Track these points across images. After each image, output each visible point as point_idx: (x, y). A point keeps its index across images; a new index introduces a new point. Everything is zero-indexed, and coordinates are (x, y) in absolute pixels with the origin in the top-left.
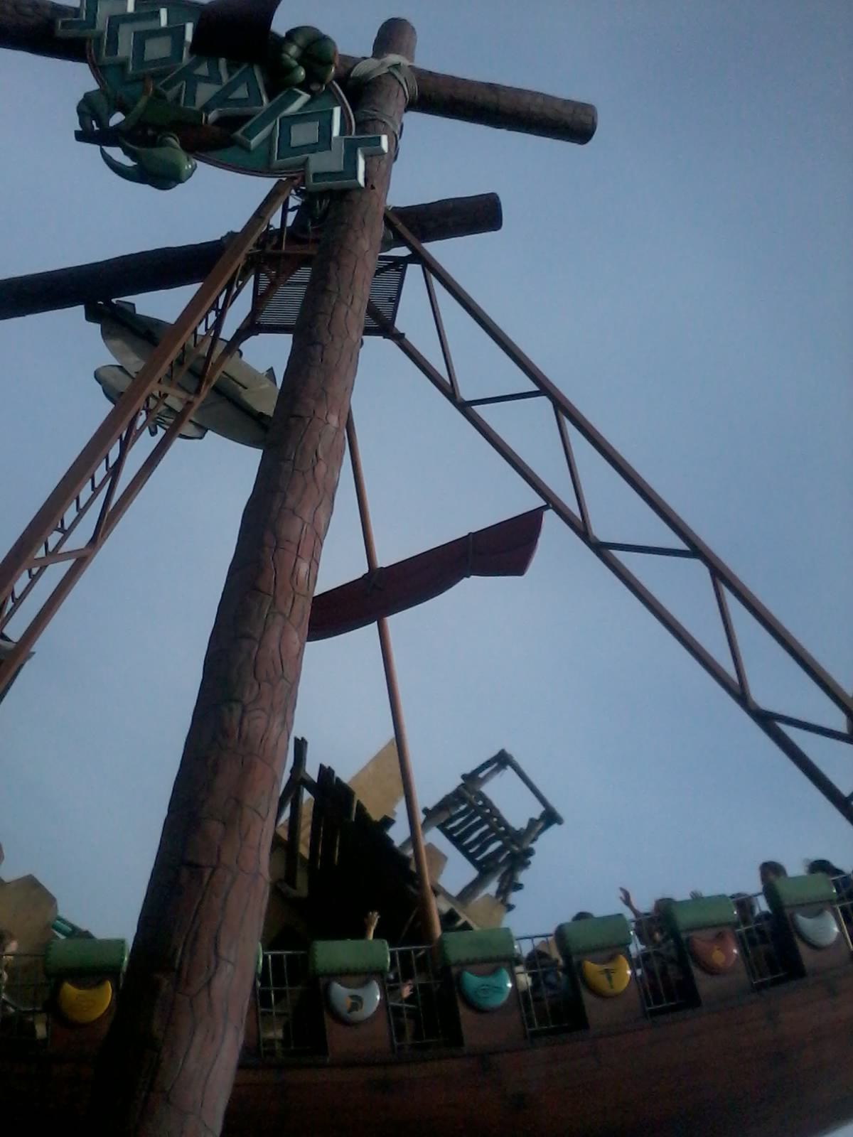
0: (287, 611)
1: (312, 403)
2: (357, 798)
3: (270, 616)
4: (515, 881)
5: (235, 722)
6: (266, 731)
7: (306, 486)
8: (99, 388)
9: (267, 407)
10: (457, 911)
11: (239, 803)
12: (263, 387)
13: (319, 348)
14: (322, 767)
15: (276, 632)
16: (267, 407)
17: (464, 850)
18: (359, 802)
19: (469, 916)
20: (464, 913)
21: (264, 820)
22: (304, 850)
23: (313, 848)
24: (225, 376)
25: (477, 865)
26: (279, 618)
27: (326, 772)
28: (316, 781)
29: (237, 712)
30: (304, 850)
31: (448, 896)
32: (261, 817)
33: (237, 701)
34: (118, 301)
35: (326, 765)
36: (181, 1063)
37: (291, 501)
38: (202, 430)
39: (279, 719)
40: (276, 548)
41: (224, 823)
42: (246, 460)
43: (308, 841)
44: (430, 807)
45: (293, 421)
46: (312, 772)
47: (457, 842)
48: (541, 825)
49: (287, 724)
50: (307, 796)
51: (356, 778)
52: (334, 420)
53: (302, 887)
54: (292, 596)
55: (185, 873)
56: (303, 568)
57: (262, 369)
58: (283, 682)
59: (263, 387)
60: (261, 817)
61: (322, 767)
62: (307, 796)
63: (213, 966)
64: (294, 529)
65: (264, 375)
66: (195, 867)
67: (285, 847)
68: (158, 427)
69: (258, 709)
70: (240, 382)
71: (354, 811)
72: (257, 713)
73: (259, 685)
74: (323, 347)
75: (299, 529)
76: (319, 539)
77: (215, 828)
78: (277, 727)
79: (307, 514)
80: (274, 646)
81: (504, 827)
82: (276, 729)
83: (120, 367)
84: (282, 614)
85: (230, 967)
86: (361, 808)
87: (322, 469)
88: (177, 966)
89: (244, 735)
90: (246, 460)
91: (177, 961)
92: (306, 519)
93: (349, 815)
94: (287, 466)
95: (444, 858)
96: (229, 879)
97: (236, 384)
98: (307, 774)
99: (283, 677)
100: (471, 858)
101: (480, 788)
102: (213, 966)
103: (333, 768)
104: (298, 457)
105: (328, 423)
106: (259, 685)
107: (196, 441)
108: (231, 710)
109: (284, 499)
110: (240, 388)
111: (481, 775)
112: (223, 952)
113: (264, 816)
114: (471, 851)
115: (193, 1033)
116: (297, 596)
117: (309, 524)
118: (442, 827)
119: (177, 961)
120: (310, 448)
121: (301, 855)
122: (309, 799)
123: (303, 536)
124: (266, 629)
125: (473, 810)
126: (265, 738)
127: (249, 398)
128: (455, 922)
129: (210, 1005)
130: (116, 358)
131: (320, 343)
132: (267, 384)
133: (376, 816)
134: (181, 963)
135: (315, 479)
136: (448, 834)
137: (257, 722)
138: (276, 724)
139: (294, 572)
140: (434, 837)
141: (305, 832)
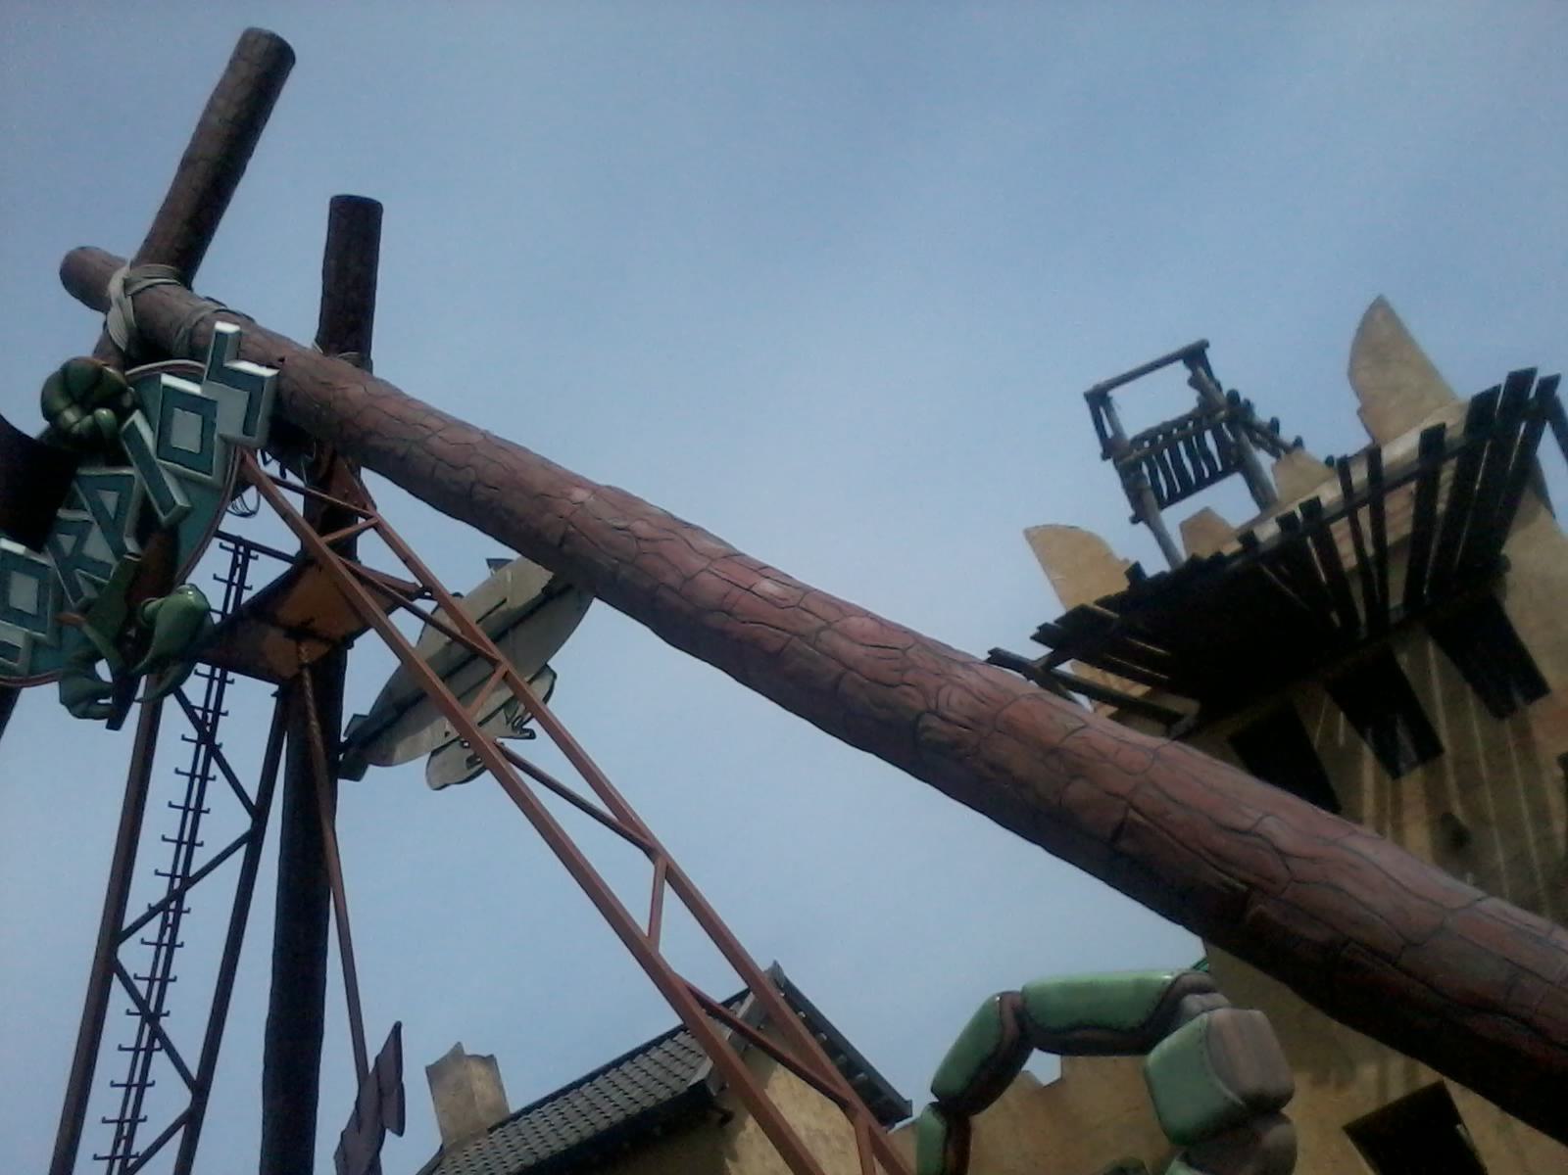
0: (819, 623)
5: (945, 727)
7: (659, 555)
9: (538, 578)
10: (1280, 514)
11: (1054, 751)
13: (479, 488)
14: (1035, 638)
15: (843, 645)
16: (538, 578)
17: (1202, 483)
18: (1098, 603)
22: (1138, 690)
25: (1226, 472)
26: (825, 635)
27: (1044, 635)
28: (1050, 650)
30: (1138, 690)
33: (919, 716)
34: (345, 735)
35: (1034, 631)
37: (671, 579)
38: (544, 671)
39: (959, 671)
40: (729, 613)
42: (601, 617)
43: (1127, 682)
44: (1131, 512)
45: (566, 548)
46: (1037, 652)
47: (1189, 489)
48: (1201, 371)
49: (967, 662)
50: (1066, 668)
51: (1062, 599)
53: (1186, 706)
55: (1125, 844)
56: (767, 587)
57: (486, 573)
60: (1083, 727)
61: (1035, 638)
62: (1066, 668)
63: (1257, 840)
64: (711, 585)
66: (1120, 830)
67: (1127, 710)
68: (525, 727)
69: (937, 694)
72: (944, 693)
76: (732, 556)
77: (1078, 790)
79: (697, 563)
80: (860, 651)
81: (1190, 420)
82: (970, 678)
83: (435, 753)
84: (822, 629)
86: (1105, 602)
87: (641, 528)
88: (1244, 887)
89: (966, 722)
90: (601, 617)
91: (1238, 885)
94: (625, 572)
99: (904, 651)
100: (1216, 477)
103: (1040, 623)
105: (582, 503)
108: (928, 728)
109: (670, 588)
110: (503, 608)
111: (1110, 432)
112: (1246, 824)
113: (1082, 724)
114: (1207, 474)
115: (1338, 889)
116: (802, 605)
117: (710, 564)
118: (1163, 504)
119: (1238, 885)
122: (1072, 666)
123: (724, 576)
125: (1154, 457)
127: (519, 600)
129: (1312, 859)
130: (420, 756)
131: (473, 484)
132: (507, 573)
133: (1122, 585)
134: (1242, 882)
136: (1174, 498)
137: (955, 701)
140: (1173, 517)
141: (1114, 682)
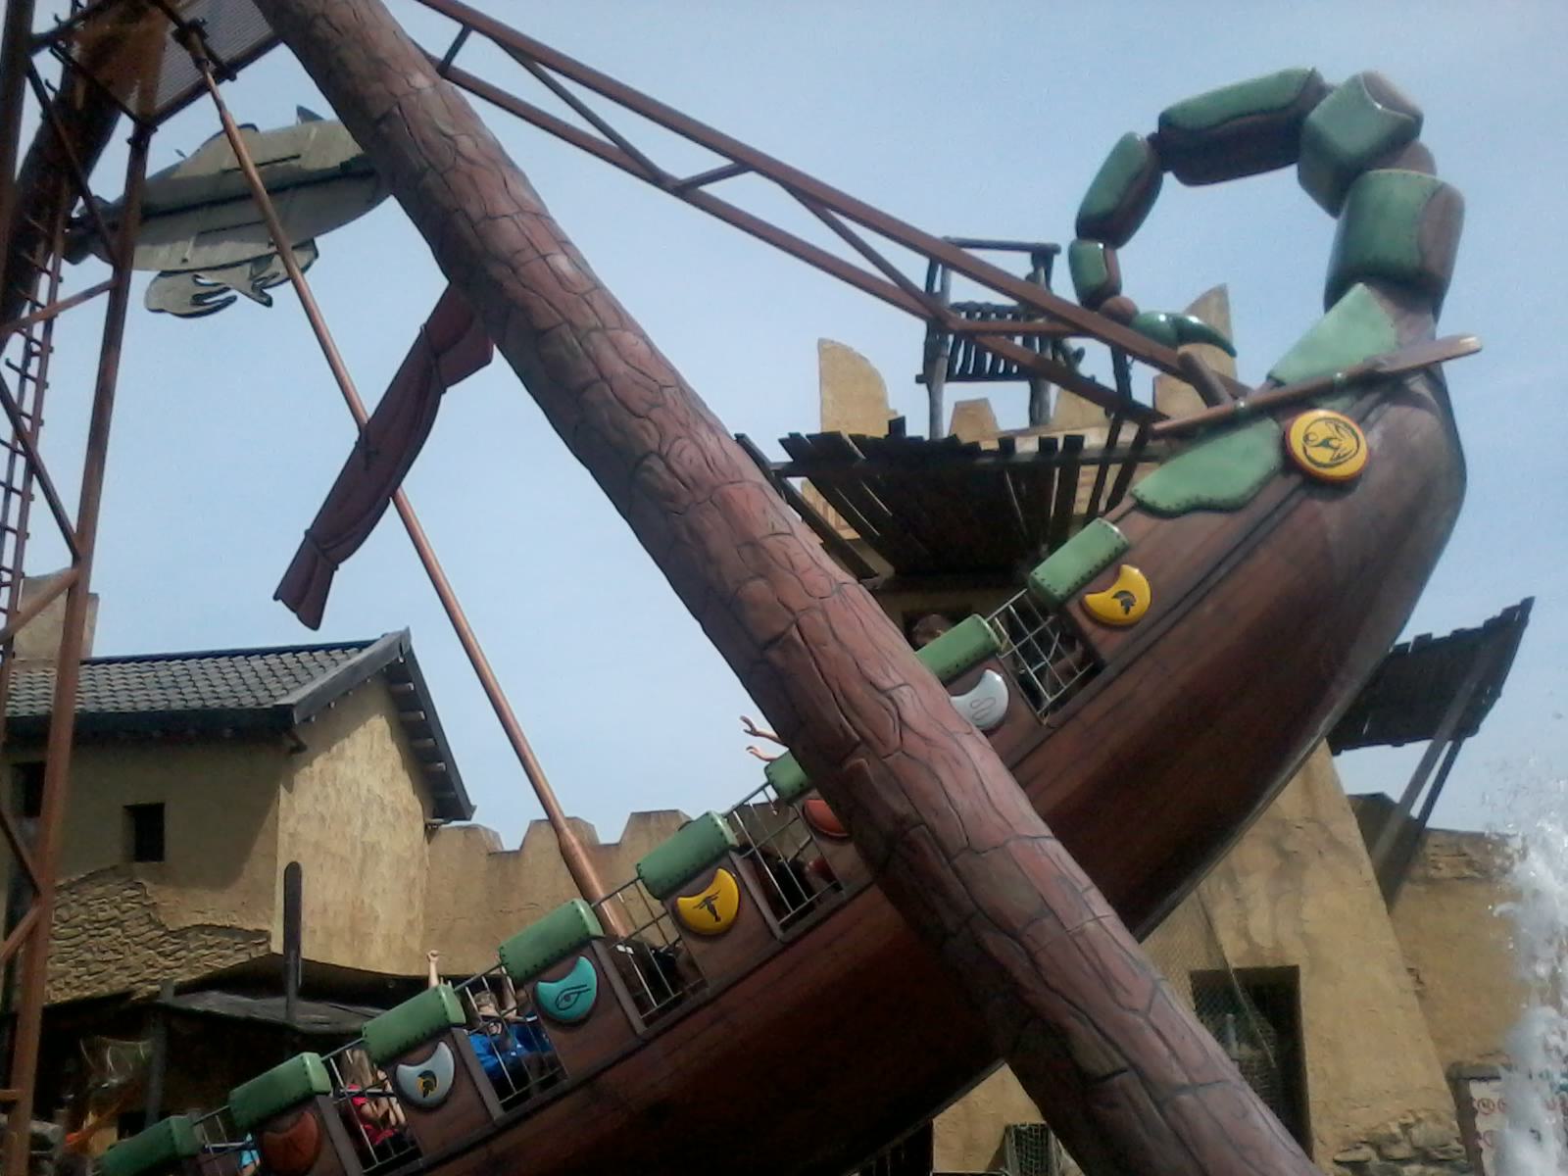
0: (593, 321)
1: (377, 88)
2: (846, 436)
3: (585, 344)
4: (1071, 353)
5: (666, 476)
6: (702, 451)
7: (470, 177)
8: (167, 317)
9: (345, 148)
10: (1045, 435)
11: (753, 544)
12: (313, 136)
13: (321, 23)
14: (782, 442)
15: (608, 354)
16: (345, 148)
17: (993, 376)
18: (851, 436)
19: (1062, 430)
20: (1054, 431)
21: (791, 534)
22: (848, 534)
23: (854, 523)
24: (263, 168)
25: (1018, 377)
26: (595, 336)
27: (791, 443)
28: (790, 460)
29: (659, 466)
30: (848, 534)
31: (1023, 433)
32: (789, 534)
33: (646, 456)
34: (78, 212)
35: (785, 435)
36: (952, 811)
37: (474, 210)
38: (308, 245)
39: (703, 431)
40: (515, 271)
41: (762, 576)
42: (389, 218)
43: (843, 522)
44: (920, 371)
45: (384, 128)
46: (778, 456)
47: (979, 375)
48: (1042, 272)
49: (715, 427)
50: (797, 483)
51: (823, 419)
52: (421, 81)
53: (883, 568)
54: (583, 301)
55: (774, 655)
56: (562, 263)
57: (291, 119)
58: (667, 392)
59: (313, 136)
60: (789, 534)
61: (782, 442)
62: (797, 483)
64: (509, 234)
65: (300, 122)
66: (778, 640)
67: (832, 544)
68: (265, 291)
69: (674, 441)
70: (284, 156)
71: (856, 448)
72: (678, 444)
73: (650, 419)
74: (324, 16)
75: (515, 229)
76: (541, 216)
77: (757, 588)
78: (710, 440)
79: (504, 206)
80: (621, 368)
81: (1010, 313)
82: (711, 444)
83: (164, 274)
84: (596, 329)
85: (904, 689)
86: (858, 439)
87: (466, 144)
88: (858, 738)
89: (689, 481)
90: (389, 218)
91: (854, 734)
92: (509, 211)
93: (856, 456)
94: (430, 179)
95: (985, 401)
96: (820, 618)
97: (284, 163)
98: (776, 464)
99: (662, 387)
100: (1007, 376)
101: (948, 302)
102: (893, 709)
103: (794, 431)
104: (432, 159)
105: (419, 90)
106: (650, 419)
107: (316, 264)
108: (650, 469)
109: (467, 216)
110: (294, 162)
111: (937, 288)
112: (886, 684)
113: (788, 530)
114: (1001, 369)
115: (935, 776)
116: (587, 297)
117: (517, 213)
118: (951, 377)
119: (854, 734)
120: (430, 135)
121: (849, 540)
122: (803, 483)
123: (527, 233)
124: (595, 360)
126: (709, 459)
127: (314, 163)
128: (1056, 448)
129: (924, 738)
130: (147, 269)
131: (316, 16)
132: (314, 130)
133: (880, 431)
134: (858, 732)
135: (471, 162)
136: (963, 377)
137: (686, 456)
138: (704, 435)
139: (560, 278)
140: (954, 393)
141: (832, 517)
